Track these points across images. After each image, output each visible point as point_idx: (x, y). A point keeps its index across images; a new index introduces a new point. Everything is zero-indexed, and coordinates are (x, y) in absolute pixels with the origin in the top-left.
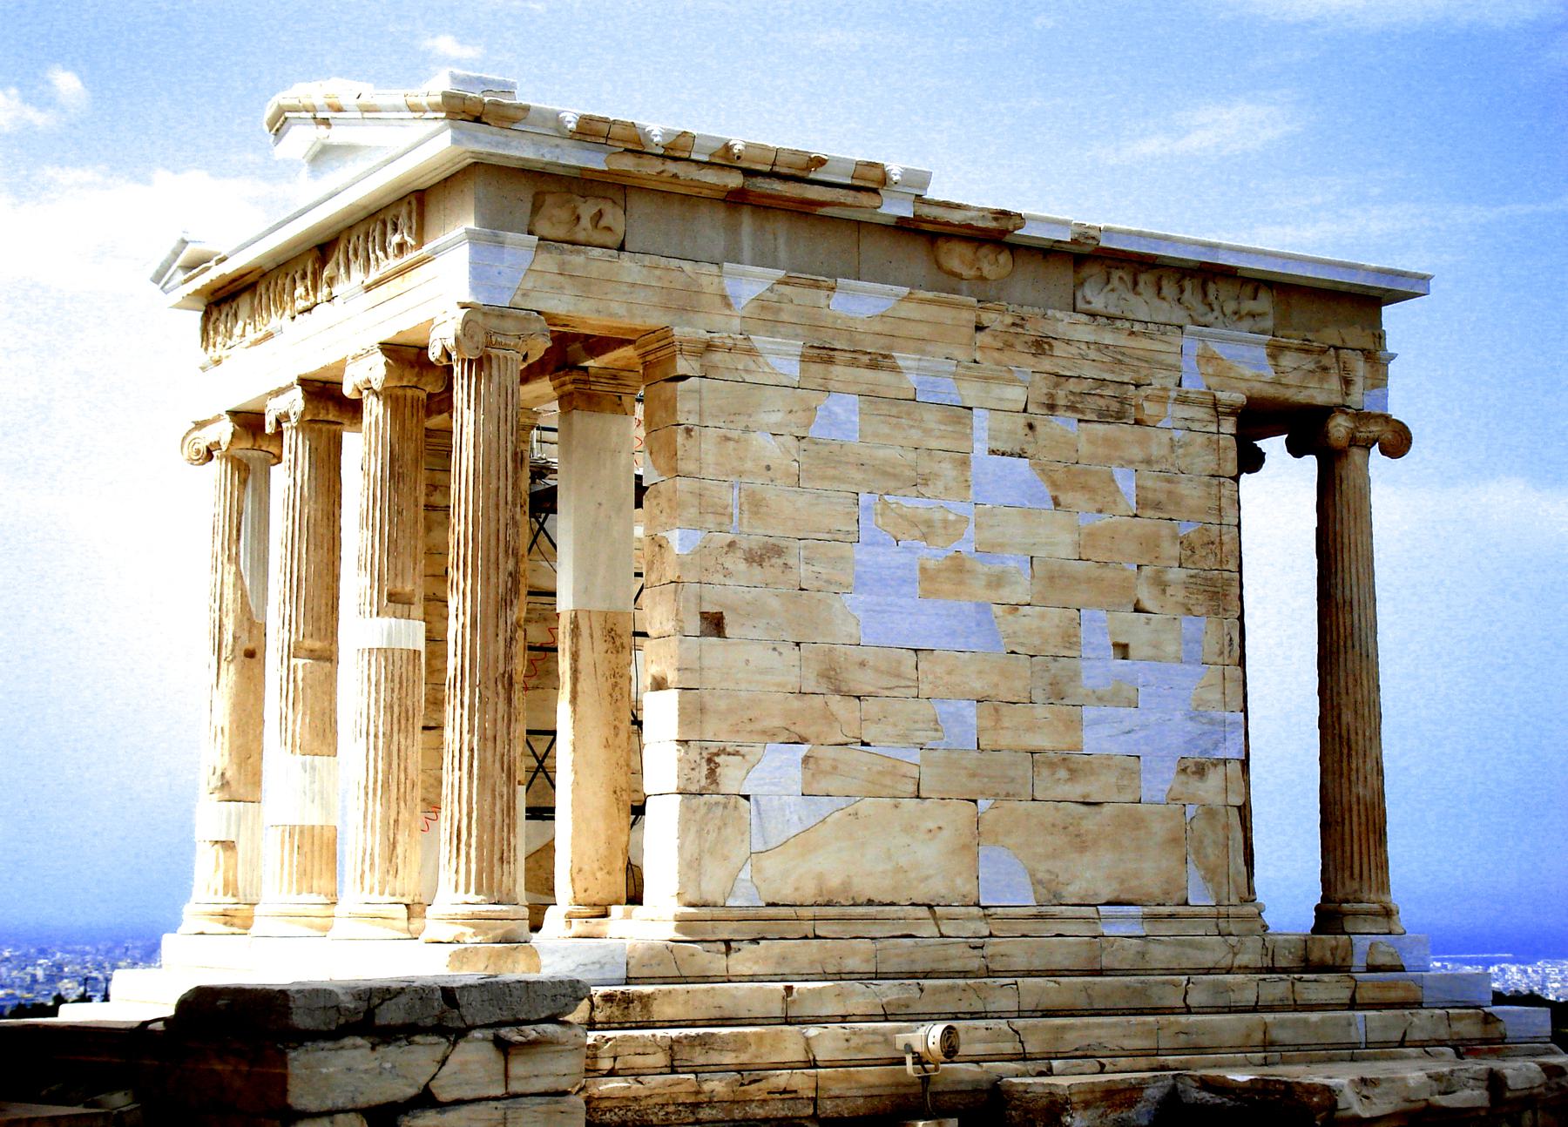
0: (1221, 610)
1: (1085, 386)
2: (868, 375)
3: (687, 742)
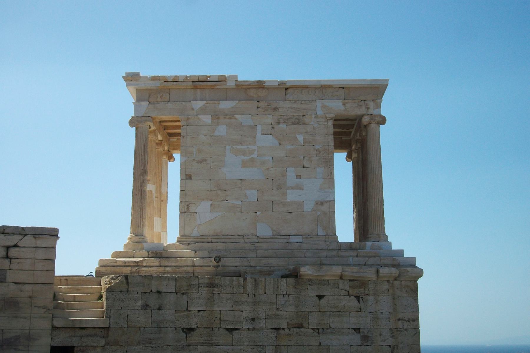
0: (328, 166)
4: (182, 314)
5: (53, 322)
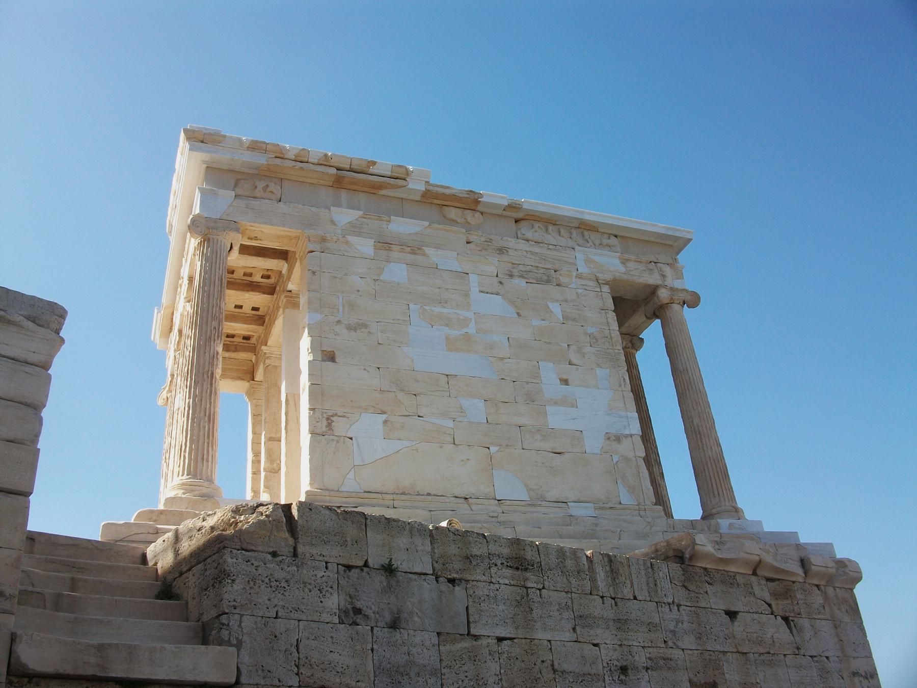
0: (617, 367)
2: (412, 256)
3: (314, 409)
5: (15, 647)
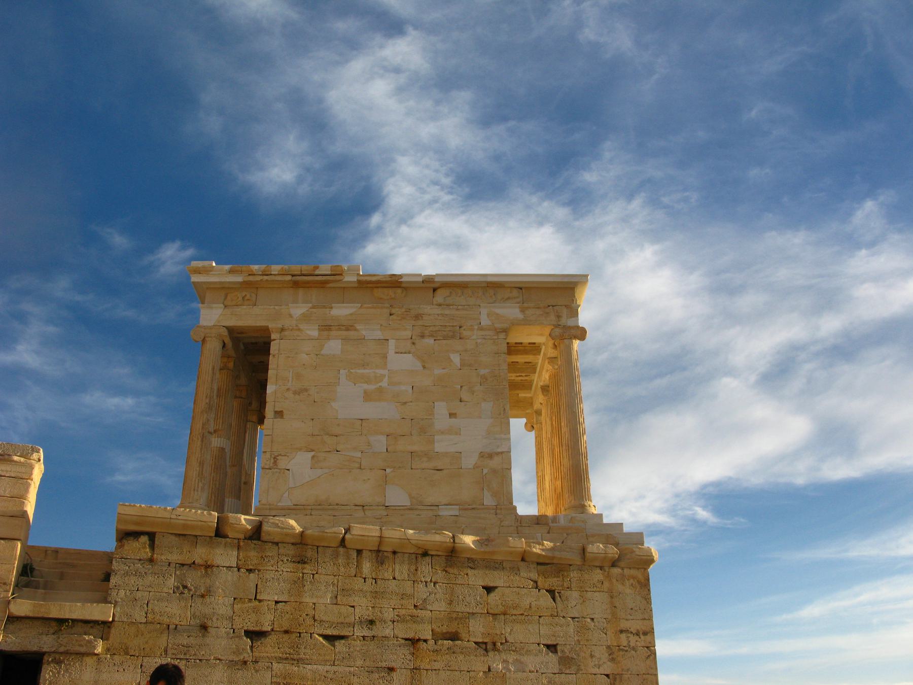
1: (437, 328)
2: (345, 333)
4: (246, 605)
